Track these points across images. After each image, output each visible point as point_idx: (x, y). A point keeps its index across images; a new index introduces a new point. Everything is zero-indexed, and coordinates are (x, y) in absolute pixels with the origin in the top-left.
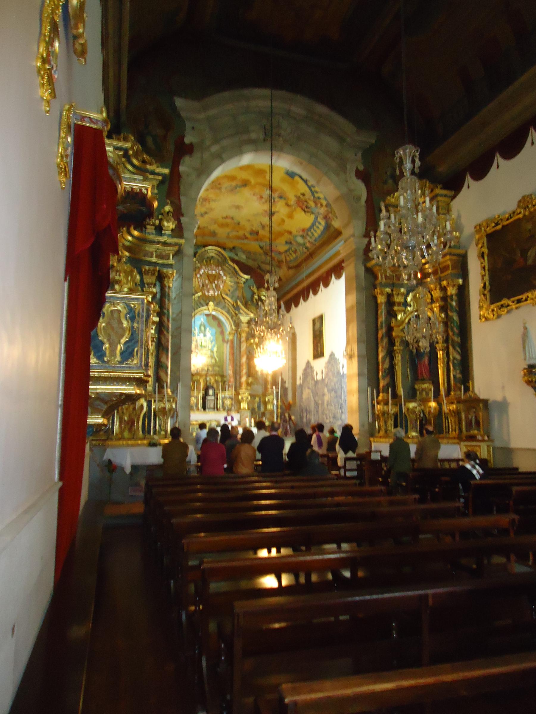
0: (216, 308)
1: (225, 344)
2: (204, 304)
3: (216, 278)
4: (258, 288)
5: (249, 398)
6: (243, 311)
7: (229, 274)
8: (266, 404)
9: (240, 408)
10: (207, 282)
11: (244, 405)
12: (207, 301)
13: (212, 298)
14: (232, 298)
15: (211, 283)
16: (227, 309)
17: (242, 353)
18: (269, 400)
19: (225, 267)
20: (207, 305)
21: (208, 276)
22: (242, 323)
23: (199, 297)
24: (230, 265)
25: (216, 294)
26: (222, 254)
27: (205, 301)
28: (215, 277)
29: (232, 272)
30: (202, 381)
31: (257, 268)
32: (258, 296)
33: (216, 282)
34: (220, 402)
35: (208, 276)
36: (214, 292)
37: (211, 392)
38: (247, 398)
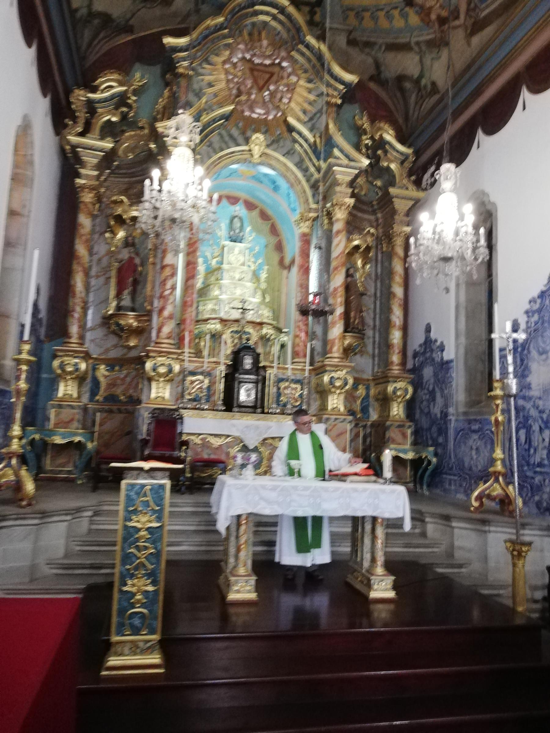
0: (269, 151)
1: (285, 272)
2: (240, 139)
3: (275, 78)
4: (373, 120)
5: (351, 381)
6: (342, 151)
7: (306, 71)
8: (385, 401)
9: (323, 408)
10: (249, 83)
11: (336, 402)
12: (249, 133)
13: (261, 126)
14: (311, 130)
15: (261, 89)
16: (297, 159)
17: (334, 264)
18: (394, 392)
19: (293, 53)
20: (247, 141)
21: (252, 70)
22: (335, 183)
23: (227, 117)
24: (308, 46)
25: (271, 117)
26: (289, 17)
27: (243, 133)
28: (272, 74)
29: (314, 67)
30: (227, 336)
31: (372, 78)
32: (372, 138)
33: (272, 88)
34: (271, 390)
35: (253, 69)
36: (267, 113)
37: (248, 362)
38: (346, 384)
